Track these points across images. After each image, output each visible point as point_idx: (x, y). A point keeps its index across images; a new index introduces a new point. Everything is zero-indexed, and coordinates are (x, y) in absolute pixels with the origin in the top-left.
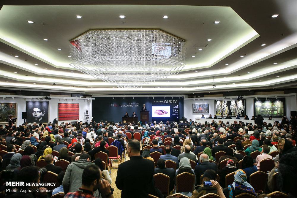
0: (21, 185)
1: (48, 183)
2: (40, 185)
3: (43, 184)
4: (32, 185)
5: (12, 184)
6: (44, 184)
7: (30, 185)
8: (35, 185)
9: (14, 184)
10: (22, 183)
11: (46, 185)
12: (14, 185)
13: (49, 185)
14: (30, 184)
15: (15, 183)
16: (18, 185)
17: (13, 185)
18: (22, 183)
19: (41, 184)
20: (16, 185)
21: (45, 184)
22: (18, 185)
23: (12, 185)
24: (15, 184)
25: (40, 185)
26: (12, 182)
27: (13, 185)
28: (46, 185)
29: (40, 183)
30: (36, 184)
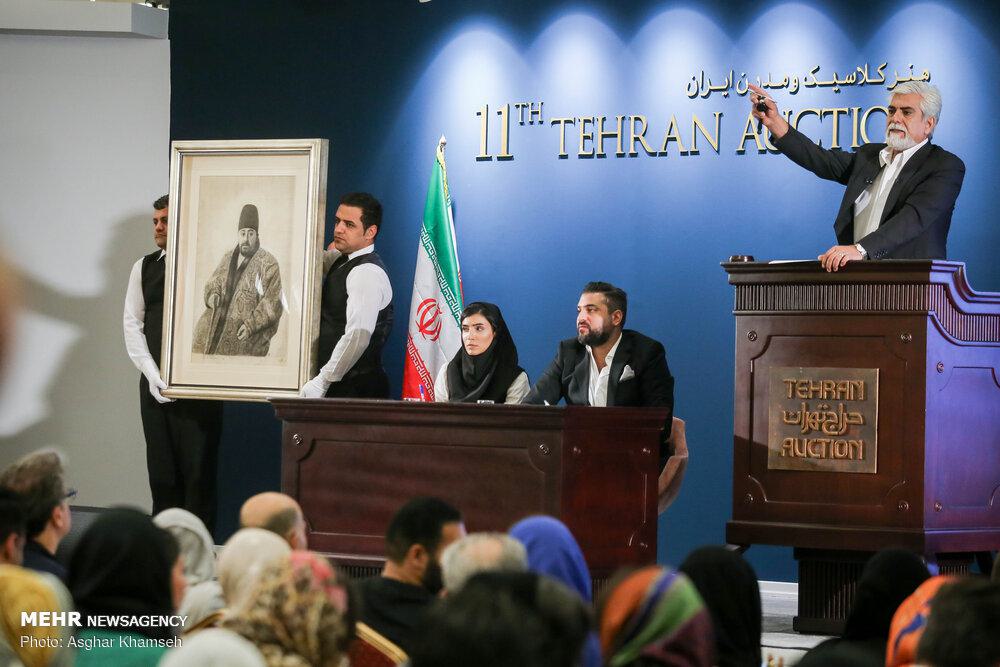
0: (71, 624)
1: (161, 617)
2: (134, 625)
3: (144, 619)
4: (106, 623)
5: (42, 619)
6: (150, 620)
7: (102, 623)
8: (119, 625)
9: (48, 619)
10: (74, 616)
11: (155, 623)
12: (48, 625)
13: (167, 625)
14: (100, 620)
15: (51, 616)
16: (59, 622)
17: (45, 622)
18: (74, 616)
19: (138, 618)
20: (55, 624)
21: (152, 620)
22: (59, 622)
23: (42, 624)
24: (50, 621)
25: (134, 625)
26: (42, 614)
27: (45, 622)
28: (155, 623)
29: (134, 617)
30: (120, 621)
